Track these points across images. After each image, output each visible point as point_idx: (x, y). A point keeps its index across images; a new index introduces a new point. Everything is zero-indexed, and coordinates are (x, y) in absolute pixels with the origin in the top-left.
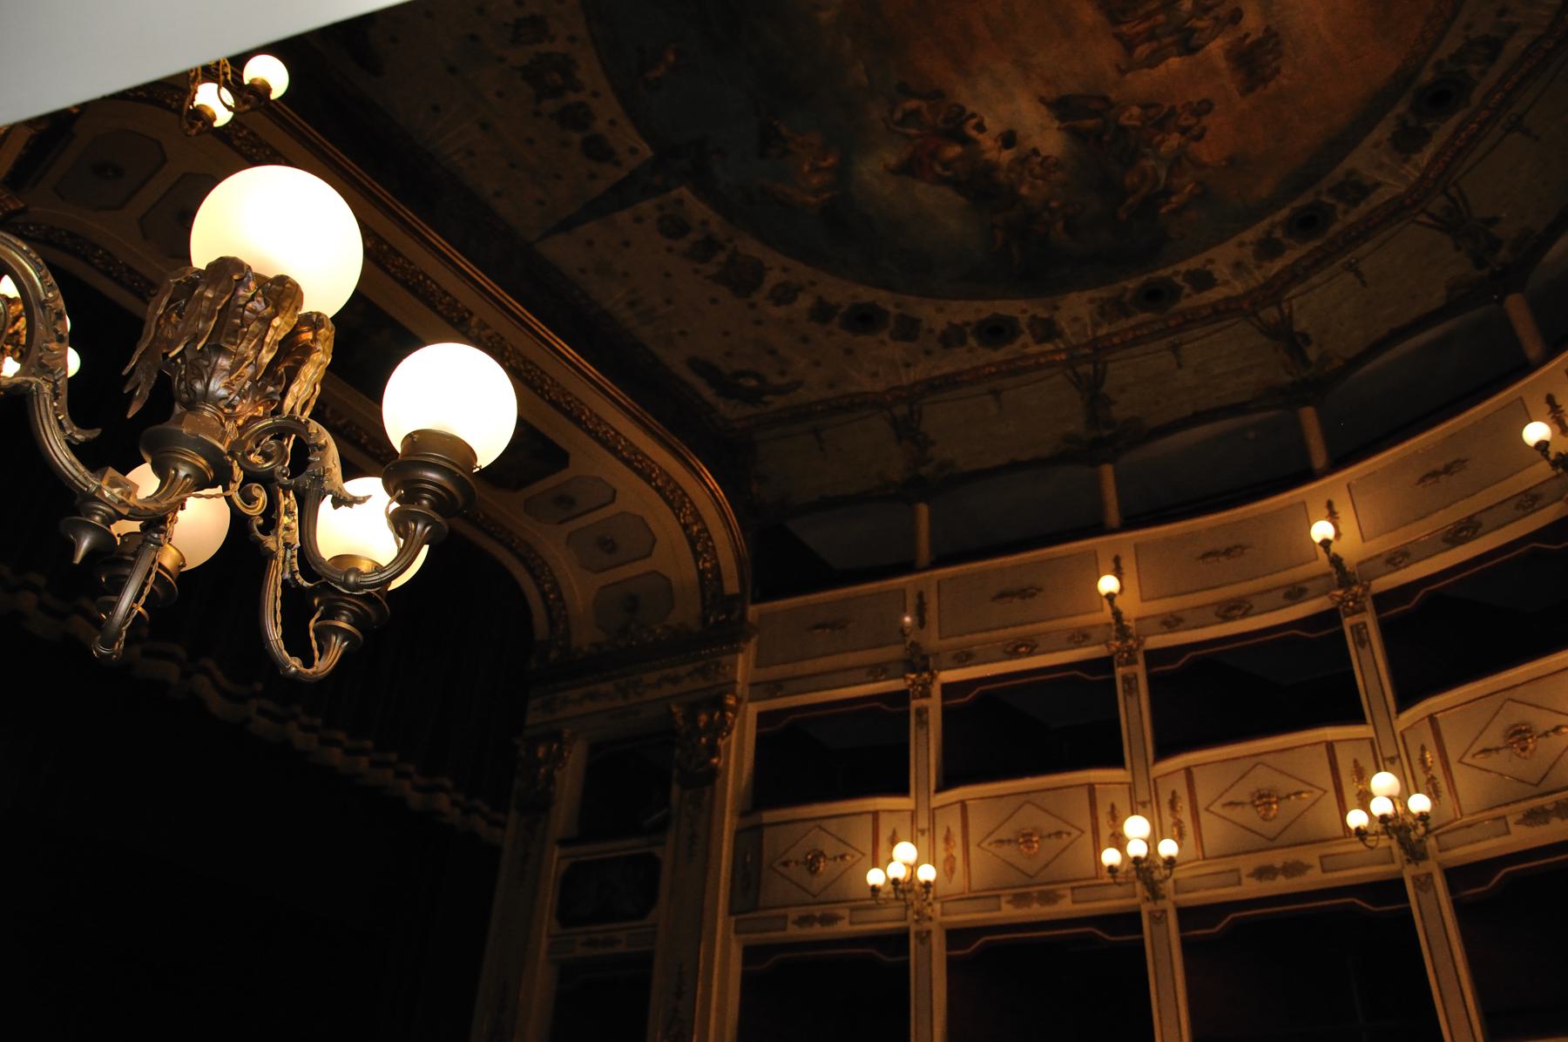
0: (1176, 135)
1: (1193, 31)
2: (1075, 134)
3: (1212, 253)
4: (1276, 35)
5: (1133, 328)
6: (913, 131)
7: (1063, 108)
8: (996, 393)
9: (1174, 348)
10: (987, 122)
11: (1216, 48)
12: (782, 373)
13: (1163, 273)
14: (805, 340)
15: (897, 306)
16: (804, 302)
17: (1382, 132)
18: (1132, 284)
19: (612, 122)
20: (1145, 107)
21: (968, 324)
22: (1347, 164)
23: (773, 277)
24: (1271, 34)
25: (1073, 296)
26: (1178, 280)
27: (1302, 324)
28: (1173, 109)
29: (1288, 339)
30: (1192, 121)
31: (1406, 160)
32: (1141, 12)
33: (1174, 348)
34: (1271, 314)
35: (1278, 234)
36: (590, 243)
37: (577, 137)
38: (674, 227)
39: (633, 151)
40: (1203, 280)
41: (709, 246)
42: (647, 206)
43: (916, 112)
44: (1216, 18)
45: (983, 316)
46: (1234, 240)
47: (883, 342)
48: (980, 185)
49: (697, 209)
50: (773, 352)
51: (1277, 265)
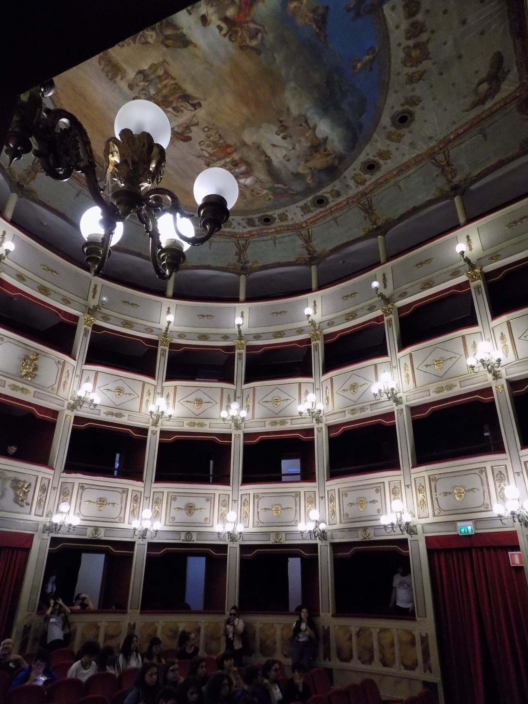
4: (110, 79)
6: (252, 26)
7: (184, 42)
10: (217, 31)
19: (397, 27)
20: (147, 43)
24: (112, 79)
32: (168, 88)
43: (252, 38)
44: (138, 86)
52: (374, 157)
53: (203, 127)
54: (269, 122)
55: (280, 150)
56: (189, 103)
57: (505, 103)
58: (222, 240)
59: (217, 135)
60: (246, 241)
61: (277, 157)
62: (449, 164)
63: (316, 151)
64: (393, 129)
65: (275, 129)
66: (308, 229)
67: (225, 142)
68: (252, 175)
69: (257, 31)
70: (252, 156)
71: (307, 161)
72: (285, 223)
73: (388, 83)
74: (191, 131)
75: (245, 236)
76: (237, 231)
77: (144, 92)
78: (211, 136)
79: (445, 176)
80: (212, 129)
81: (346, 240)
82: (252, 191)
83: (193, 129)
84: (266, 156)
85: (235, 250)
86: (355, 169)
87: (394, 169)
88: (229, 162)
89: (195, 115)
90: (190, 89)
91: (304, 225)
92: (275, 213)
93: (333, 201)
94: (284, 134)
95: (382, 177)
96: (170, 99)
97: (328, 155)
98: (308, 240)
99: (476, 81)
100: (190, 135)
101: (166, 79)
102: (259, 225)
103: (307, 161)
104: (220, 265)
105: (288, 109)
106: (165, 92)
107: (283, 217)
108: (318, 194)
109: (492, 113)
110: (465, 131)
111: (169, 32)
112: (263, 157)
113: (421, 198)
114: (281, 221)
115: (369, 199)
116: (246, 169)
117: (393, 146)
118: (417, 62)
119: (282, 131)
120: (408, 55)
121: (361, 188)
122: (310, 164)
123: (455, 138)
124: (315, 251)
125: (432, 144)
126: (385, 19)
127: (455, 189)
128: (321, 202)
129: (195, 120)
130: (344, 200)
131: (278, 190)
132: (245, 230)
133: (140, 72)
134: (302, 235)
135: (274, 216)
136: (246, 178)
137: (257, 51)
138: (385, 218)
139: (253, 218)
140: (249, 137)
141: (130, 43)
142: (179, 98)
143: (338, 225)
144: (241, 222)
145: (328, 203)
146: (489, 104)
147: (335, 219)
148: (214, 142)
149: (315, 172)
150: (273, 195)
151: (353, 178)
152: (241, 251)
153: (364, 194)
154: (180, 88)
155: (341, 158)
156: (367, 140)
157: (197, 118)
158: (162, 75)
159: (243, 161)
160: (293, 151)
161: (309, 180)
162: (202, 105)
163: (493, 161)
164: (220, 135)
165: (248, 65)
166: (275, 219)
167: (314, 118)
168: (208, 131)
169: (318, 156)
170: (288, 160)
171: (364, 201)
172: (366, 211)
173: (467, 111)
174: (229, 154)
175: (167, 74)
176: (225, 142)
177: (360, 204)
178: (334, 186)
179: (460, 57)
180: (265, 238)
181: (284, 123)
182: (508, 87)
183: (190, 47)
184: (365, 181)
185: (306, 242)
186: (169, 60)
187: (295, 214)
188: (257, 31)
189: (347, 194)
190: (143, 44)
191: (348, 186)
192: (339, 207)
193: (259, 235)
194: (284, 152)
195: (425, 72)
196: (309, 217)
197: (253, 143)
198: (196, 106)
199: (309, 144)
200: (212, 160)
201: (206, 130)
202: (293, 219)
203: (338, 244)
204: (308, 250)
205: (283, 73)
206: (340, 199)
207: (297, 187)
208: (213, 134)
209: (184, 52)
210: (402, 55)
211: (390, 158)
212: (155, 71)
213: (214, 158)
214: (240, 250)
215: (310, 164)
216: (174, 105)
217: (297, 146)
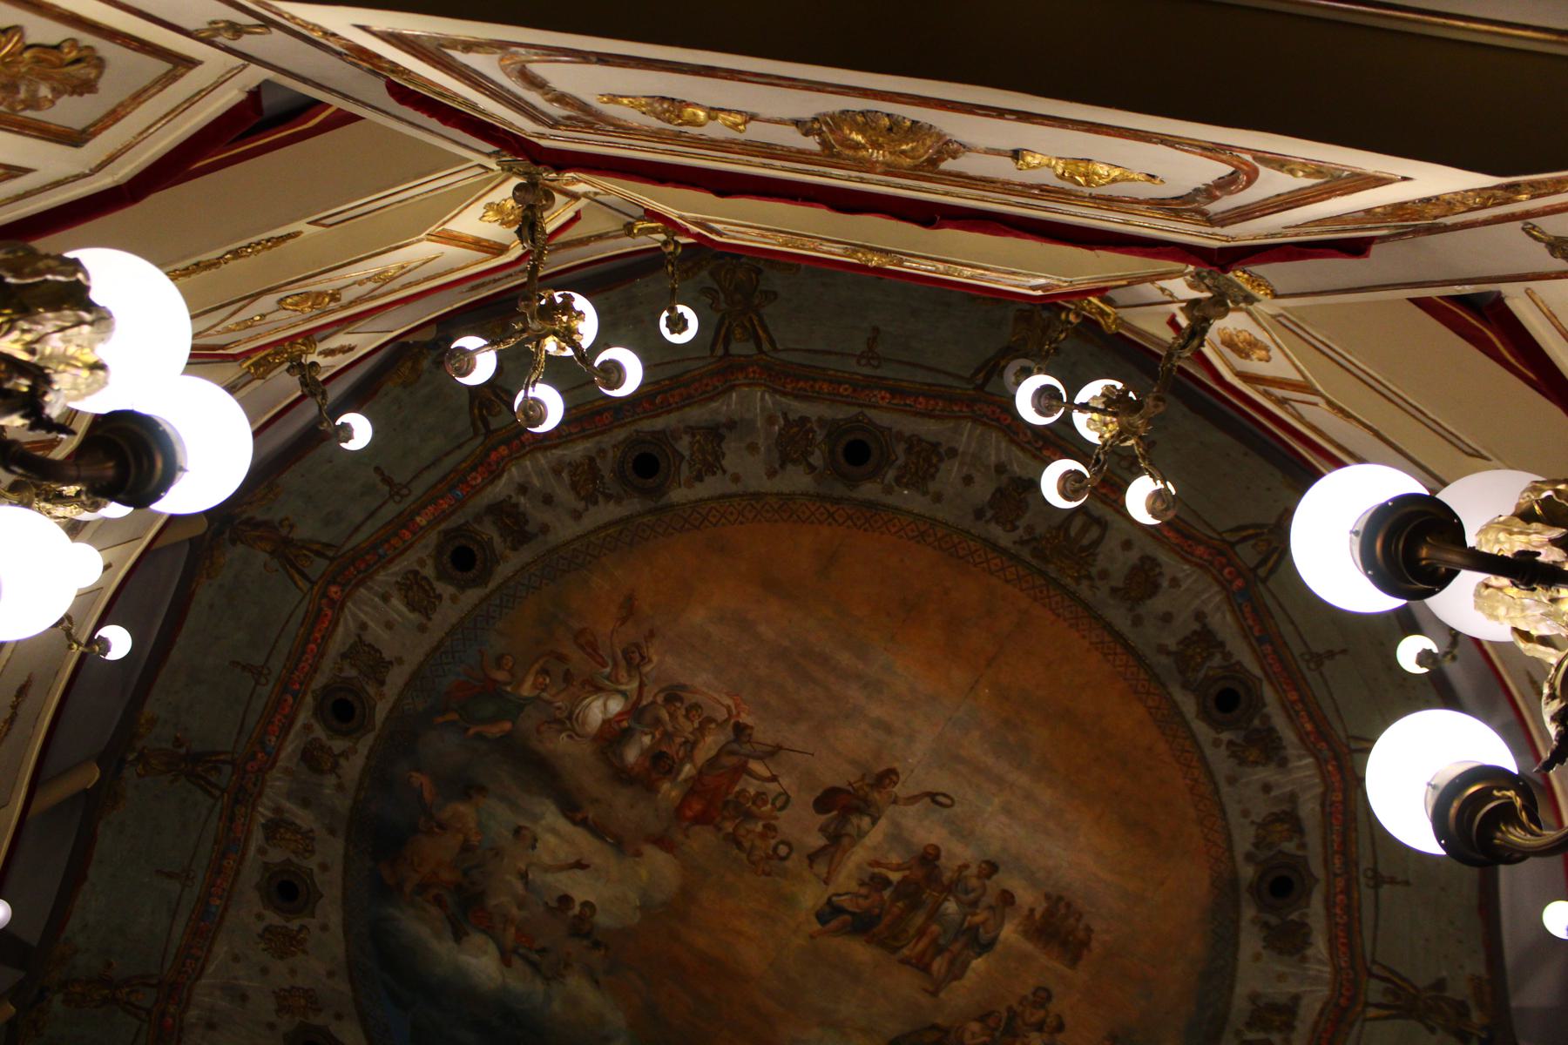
0: (1034, 1035)
1: (974, 929)
4: (1060, 898)
11: (1009, 932)
17: (1250, 942)
20: (981, 1019)
22: (1241, 990)
28: (1010, 1009)
30: (1040, 1014)
31: (1304, 959)
32: (912, 931)
52: (302, 928)
53: (794, 855)
56: (853, 914)
59: (747, 845)
60: (489, 433)
61: (554, 831)
65: (601, 919)
66: (313, 583)
67: (719, 829)
70: (623, 806)
71: (466, 848)
74: (821, 830)
75: (504, 451)
77: (972, 896)
78: (763, 836)
80: (769, 858)
81: (175, 655)
82: (568, 677)
83: (818, 841)
84: (583, 823)
87: (226, 909)
88: (682, 763)
89: (826, 882)
90: (860, 951)
91: (334, 589)
93: (307, 728)
94: (571, 913)
95: (237, 873)
96: (900, 904)
97: (422, 888)
100: (823, 818)
101: (924, 953)
102: (478, 518)
103: (466, 848)
105: (597, 982)
106: (919, 919)
107: (418, 593)
108: (369, 739)
112: (590, 816)
114: (416, 573)
115: (217, 793)
116: (621, 757)
119: (580, 918)
121: (264, 812)
124: (233, 542)
129: (821, 868)
130: (279, 749)
133: (986, 947)
134: (318, 554)
135: (451, 590)
136: (604, 722)
139: (515, 549)
141: (1021, 1003)
142: (879, 916)
143: (235, 663)
145: (318, 712)
148: (749, 816)
150: (495, 681)
151: (308, 836)
154: (882, 944)
157: (817, 876)
158: (933, 958)
159: (643, 780)
160: (522, 866)
161: (418, 779)
162: (814, 919)
164: (739, 845)
166: (442, 575)
167: (519, 982)
168: (775, 849)
169: (446, 875)
170: (518, 831)
174: (695, 788)
175: (921, 965)
176: (719, 829)
177: (224, 762)
178: (340, 787)
180: (431, 477)
181: (585, 943)
184: (267, 839)
185: (287, 542)
187: (389, 625)
189: (286, 771)
190: (989, 1014)
191: (305, 803)
194: (543, 855)
196: (341, 629)
197: (638, 854)
198: (829, 912)
199: (492, 902)
200: (732, 753)
201: (783, 850)
202: (386, 598)
203: (191, 623)
206: (292, 746)
208: (758, 842)
211: (260, 936)
212: (951, 963)
213: (729, 761)
216: (887, 894)
217: (519, 887)
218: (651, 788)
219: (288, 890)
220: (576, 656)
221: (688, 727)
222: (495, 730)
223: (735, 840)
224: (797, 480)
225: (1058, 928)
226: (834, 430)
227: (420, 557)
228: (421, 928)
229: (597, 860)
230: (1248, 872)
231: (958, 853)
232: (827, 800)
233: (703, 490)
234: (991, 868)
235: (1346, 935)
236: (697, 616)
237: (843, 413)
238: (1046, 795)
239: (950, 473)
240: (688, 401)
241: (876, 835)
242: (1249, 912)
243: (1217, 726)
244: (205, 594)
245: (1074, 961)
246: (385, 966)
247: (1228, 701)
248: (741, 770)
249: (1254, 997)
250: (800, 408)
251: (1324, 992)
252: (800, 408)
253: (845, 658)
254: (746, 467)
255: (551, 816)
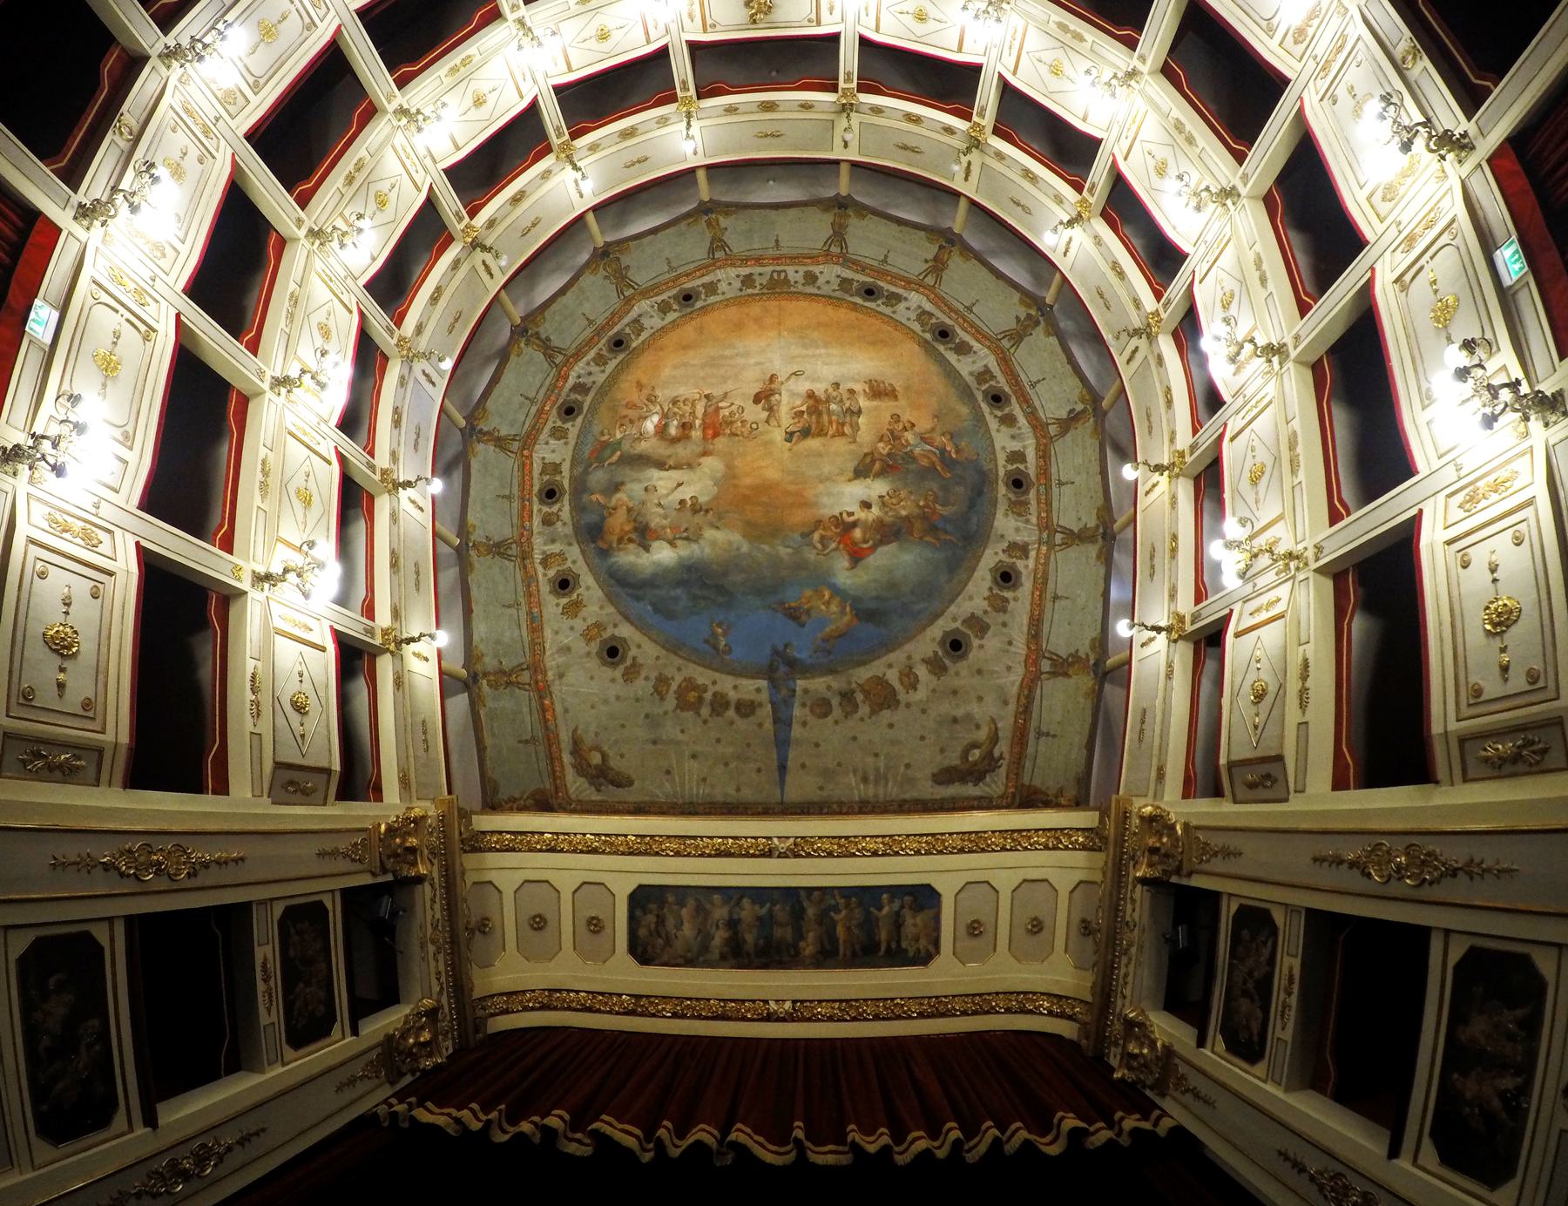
1: (849, 409)
2: (877, 475)
3: (998, 446)
5: (1039, 502)
7: (860, 472)
8: (1056, 598)
9: (1060, 484)
11: (863, 402)
12: (978, 727)
13: (1001, 472)
14: (955, 692)
15: (954, 619)
16: (922, 672)
17: (952, 357)
18: (1002, 489)
19: (735, 687)
20: (881, 440)
21: (991, 589)
23: (892, 676)
25: (996, 523)
26: (1010, 467)
27: (1063, 414)
29: (1073, 419)
33: (1060, 484)
34: (1053, 430)
35: (999, 414)
36: (803, 766)
37: (731, 713)
38: (822, 707)
39: (758, 690)
40: (1017, 457)
41: (847, 696)
42: (797, 712)
43: (822, 537)
45: (989, 577)
46: (993, 433)
47: (981, 647)
48: (888, 532)
49: (818, 684)
50: (955, 720)
51: (1022, 420)
54: (716, 498)
55: (667, 489)
57: (556, 776)
58: (582, 337)
62: (509, 684)
63: (636, 529)
64: (606, 635)
65: (702, 500)
68: (656, 433)
69: (825, 547)
70: (683, 451)
71: (629, 510)
72: (546, 430)
73: (676, 654)
76: (581, 364)
79: (495, 673)
81: (472, 492)
82: (631, 422)
83: (766, 414)
84: (671, 468)
85: (556, 341)
86: (574, 562)
90: (813, 443)
92: (573, 428)
97: (620, 540)
98: (501, 443)
99: (611, 754)
103: (629, 510)
104: (554, 307)
106: (825, 418)
107: (559, 434)
108: (567, 497)
109: (552, 759)
110: (546, 721)
111: (877, 466)
113: (480, 629)
117: (579, 624)
118: (680, 694)
120: (695, 688)
121: (538, 557)
122: (622, 512)
123: (542, 705)
125: (550, 675)
126: (753, 678)
127: (474, 677)
128: (550, 494)
129: (773, 422)
131: (608, 452)
132: (573, 374)
133: (859, 412)
137: (806, 535)
138: (477, 565)
140: (712, 465)
144: (591, 379)
145: (542, 502)
146: (567, 758)
147: (509, 497)
148: (732, 423)
149: (606, 512)
151: (561, 554)
152: (548, 348)
153: (525, 556)
154: (819, 435)
155: (605, 553)
156: (611, 598)
163: (488, 741)
165: (798, 517)
167: (685, 551)
169: (627, 528)
170: (646, 489)
171: (514, 550)
172: (498, 545)
173: (575, 731)
174: (705, 427)
179: (654, 742)
180: (543, 391)
182: (576, 785)
183: (851, 475)
185: (499, 439)
186: (853, 447)
188: (825, 547)
191: (553, 541)
192: (525, 513)
193: (553, 387)
195: (662, 699)
198: (789, 436)
199: (652, 525)
204: (488, 433)
205: (766, 548)
206: (536, 521)
207: (598, 477)
209: (851, 466)
210: (700, 681)
213: (710, 410)
214: (548, 347)
215: (622, 512)
218: (688, 437)
219: (564, 584)
220: (631, 413)
221: (688, 409)
222: (615, 458)
223: (733, 434)
224: (671, 316)
225: (879, 391)
226: (675, 297)
227: (553, 420)
228: (631, 558)
229: (685, 479)
230: (928, 336)
231: (820, 388)
232: (757, 399)
233: (641, 338)
234: (837, 385)
235: (980, 335)
236: (666, 372)
237: (675, 291)
238: (835, 352)
239: (723, 287)
240: (621, 318)
241: (785, 398)
242: (941, 348)
243: (874, 300)
244: (475, 465)
245: (896, 398)
246: (623, 585)
247: (870, 292)
248: (718, 409)
249: (971, 374)
250: (659, 299)
251: (992, 358)
252: (659, 299)
253: (728, 352)
254: (654, 322)
255: (657, 477)
